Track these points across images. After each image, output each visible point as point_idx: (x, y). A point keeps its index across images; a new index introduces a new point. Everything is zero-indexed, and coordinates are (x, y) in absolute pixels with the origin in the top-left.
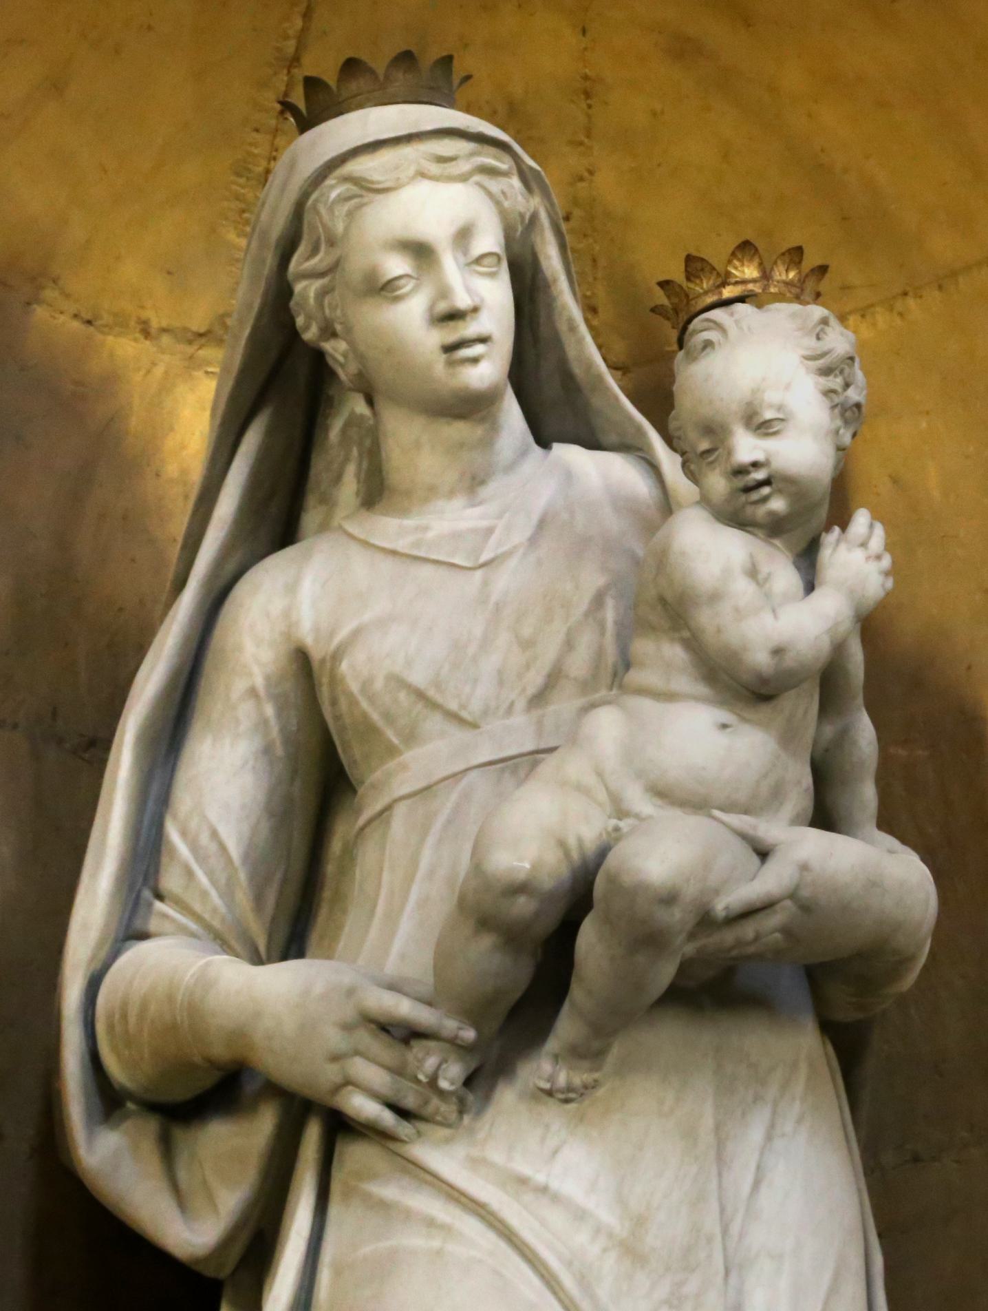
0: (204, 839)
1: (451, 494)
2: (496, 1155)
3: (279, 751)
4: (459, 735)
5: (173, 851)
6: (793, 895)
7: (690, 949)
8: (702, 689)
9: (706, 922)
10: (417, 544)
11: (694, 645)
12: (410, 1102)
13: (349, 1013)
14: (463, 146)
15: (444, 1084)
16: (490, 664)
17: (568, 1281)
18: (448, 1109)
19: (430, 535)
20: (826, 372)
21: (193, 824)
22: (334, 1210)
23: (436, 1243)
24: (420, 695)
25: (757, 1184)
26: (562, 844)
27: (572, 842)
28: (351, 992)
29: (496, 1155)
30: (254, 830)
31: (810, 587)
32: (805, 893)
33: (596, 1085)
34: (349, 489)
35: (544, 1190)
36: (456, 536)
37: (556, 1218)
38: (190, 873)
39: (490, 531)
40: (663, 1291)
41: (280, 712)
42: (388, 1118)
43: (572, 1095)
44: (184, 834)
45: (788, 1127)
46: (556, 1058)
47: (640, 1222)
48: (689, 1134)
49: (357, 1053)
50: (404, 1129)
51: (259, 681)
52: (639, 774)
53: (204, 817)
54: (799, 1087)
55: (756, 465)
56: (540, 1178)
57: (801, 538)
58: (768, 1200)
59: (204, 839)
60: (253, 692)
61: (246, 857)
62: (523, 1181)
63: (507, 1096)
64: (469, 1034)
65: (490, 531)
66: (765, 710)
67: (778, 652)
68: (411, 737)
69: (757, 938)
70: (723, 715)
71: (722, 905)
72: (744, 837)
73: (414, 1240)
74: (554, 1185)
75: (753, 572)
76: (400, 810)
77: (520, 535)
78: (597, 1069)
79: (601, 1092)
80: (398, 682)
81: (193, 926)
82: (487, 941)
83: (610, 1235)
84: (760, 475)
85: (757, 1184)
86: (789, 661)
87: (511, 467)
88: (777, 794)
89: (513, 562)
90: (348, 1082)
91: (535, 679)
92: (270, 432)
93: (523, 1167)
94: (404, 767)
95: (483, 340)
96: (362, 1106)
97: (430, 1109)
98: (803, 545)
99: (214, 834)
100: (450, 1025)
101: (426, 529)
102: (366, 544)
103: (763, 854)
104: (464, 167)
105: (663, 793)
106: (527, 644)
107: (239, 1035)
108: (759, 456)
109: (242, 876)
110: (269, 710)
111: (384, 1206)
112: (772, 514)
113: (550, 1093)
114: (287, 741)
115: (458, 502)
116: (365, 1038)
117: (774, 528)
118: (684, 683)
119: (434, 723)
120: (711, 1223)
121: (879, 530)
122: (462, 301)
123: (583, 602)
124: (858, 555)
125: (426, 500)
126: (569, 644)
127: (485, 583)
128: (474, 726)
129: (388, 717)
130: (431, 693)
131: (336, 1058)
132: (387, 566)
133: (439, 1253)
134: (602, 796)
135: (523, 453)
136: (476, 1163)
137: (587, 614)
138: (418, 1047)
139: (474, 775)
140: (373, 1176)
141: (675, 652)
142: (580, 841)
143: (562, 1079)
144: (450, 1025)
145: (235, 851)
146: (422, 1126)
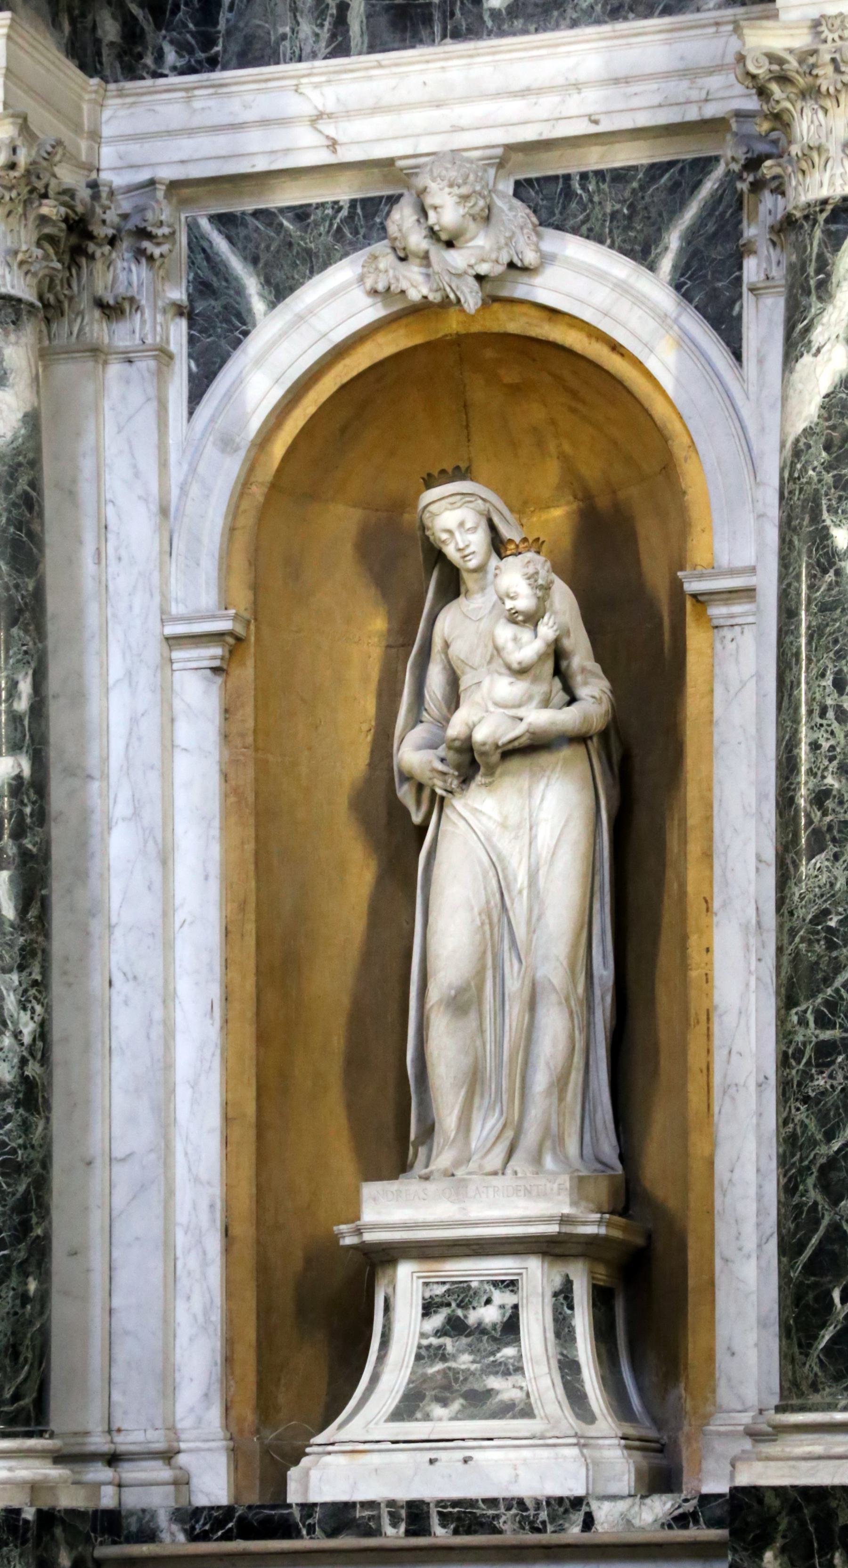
2: (470, 802)
14: (459, 497)
17: (482, 838)
28: (431, 762)
29: (470, 802)
37: (484, 820)
45: (553, 781)
47: (506, 818)
48: (520, 791)
54: (558, 769)
58: (546, 804)
63: (473, 785)
70: (512, 679)
88: (530, 698)
89: (484, 620)
95: (473, 553)
103: (521, 719)
104: (459, 504)
105: (496, 704)
116: (436, 774)
120: (526, 815)
122: (461, 546)
136: (466, 805)
144: (451, 771)
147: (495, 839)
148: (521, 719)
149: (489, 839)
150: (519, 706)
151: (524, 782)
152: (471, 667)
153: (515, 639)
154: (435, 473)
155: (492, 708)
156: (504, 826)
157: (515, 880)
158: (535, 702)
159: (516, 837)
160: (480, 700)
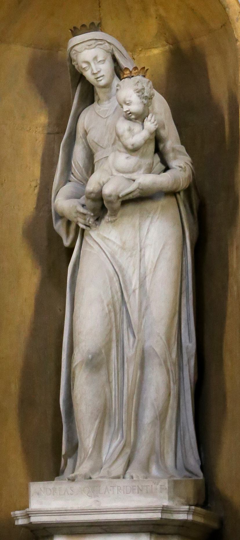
0: (77, 163)
6: (138, 188)
16: (107, 137)
20: (138, 92)
25: (148, 233)
30: (84, 161)
32: (140, 188)
33: (116, 220)
35: (108, 239)
40: (129, 254)
46: (109, 216)
47: (124, 243)
53: (76, 160)
55: (128, 111)
56: (107, 237)
58: (150, 235)
63: (103, 222)
67: (133, 145)
70: (128, 155)
71: (120, 196)
74: (110, 238)
78: (116, 217)
79: (117, 220)
80: (93, 140)
84: (128, 113)
85: (148, 233)
88: (140, 167)
92: (82, 86)
93: (105, 236)
95: (103, 76)
103: (134, 181)
105: (118, 171)
108: (128, 109)
115: (107, 102)
116: (79, 215)
117: (136, 119)
118: (122, 149)
119: (99, 148)
131: (75, 218)
136: (98, 235)
144: (89, 213)
145: (81, 166)
148: (134, 181)
149: (114, 257)
150: (133, 172)
153: (130, 130)
154: (79, 27)
155: (115, 173)
156: (123, 248)
157: (131, 283)
158: (142, 171)
159: (131, 256)
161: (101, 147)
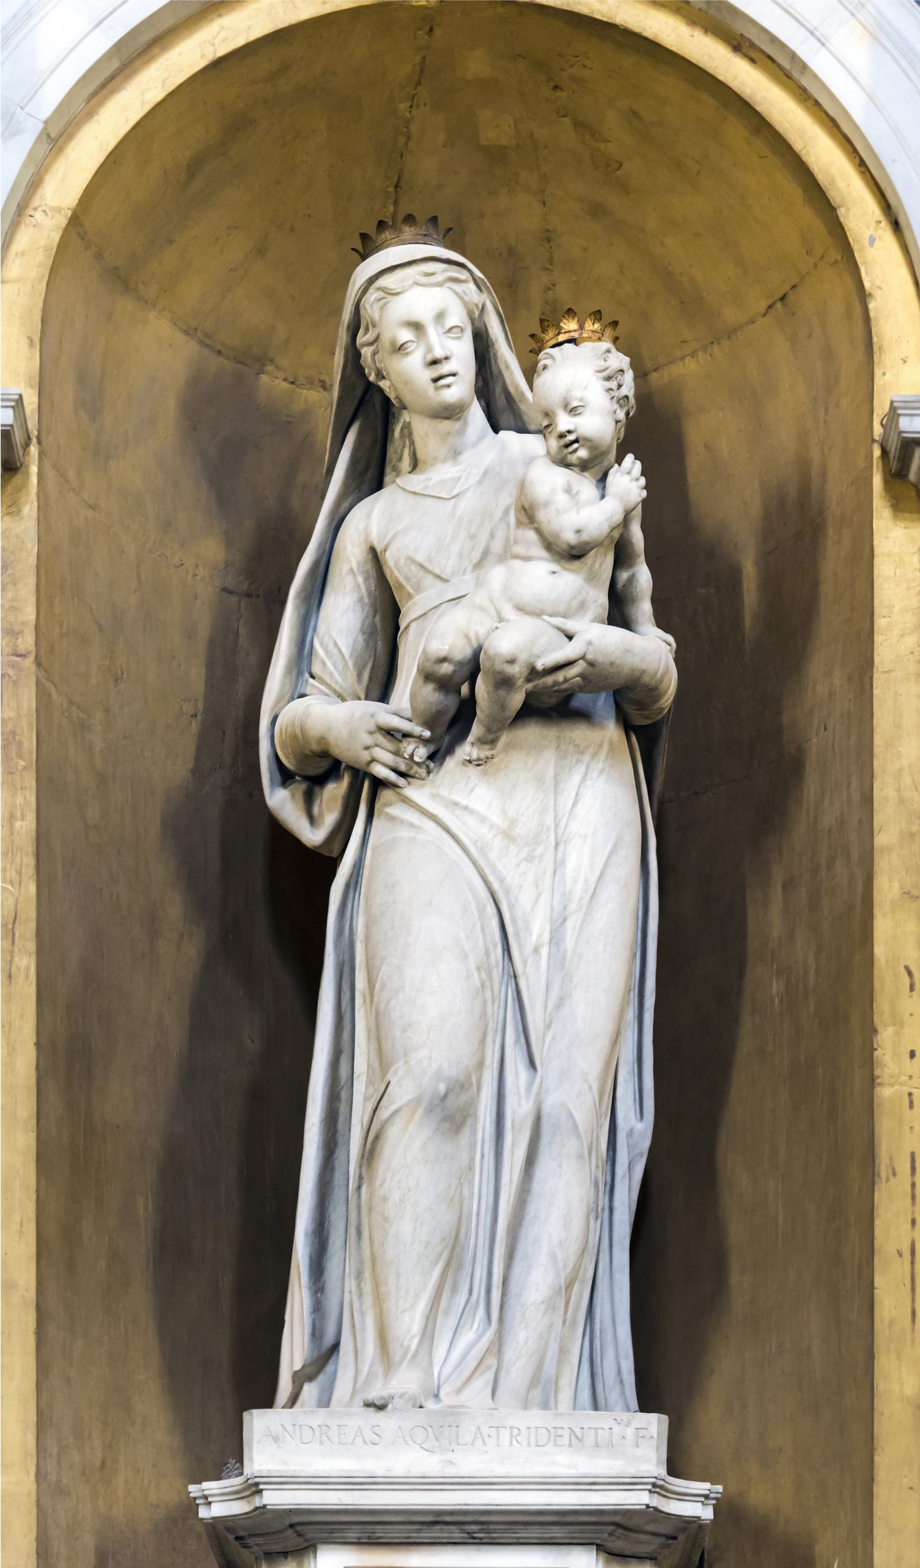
0: (331, 646)
1: (445, 460)
2: (444, 792)
3: (366, 600)
4: (439, 585)
5: (317, 654)
6: (583, 658)
7: (530, 686)
8: (544, 553)
9: (533, 673)
10: (425, 488)
11: (538, 531)
12: (403, 768)
13: (372, 727)
15: (416, 759)
16: (455, 549)
17: (473, 850)
18: (422, 772)
19: (431, 483)
21: (326, 639)
22: (375, 821)
23: (412, 835)
24: (422, 566)
26: (467, 636)
27: (472, 636)
28: (372, 716)
31: (603, 497)
32: (589, 656)
34: (406, 463)
35: (466, 808)
36: (443, 482)
37: (471, 821)
38: (324, 664)
39: (459, 478)
40: (524, 854)
41: (366, 579)
42: (393, 777)
43: (480, 762)
44: (322, 644)
47: (513, 822)
48: (540, 780)
49: (377, 745)
50: (401, 781)
51: (354, 565)
52: (510, 600)
55: (569, 432)
56: (464, 802)
57: (598, 470)
59: (331, 646)
60: (352, 570)
61: (352, 655)
62: (456, 804)
63: (451, 763)
64: (427, 734)
65: (459, 478)
66: (576, 564)
68: (418, 589)
69: (566, 681)
70: (555, 567)
71: (540, 665)
72: (559, 629)
73: (404, 833)
74: (471, 805)
75: (568, 491)
76: (413, 626)
77: (473, 481)
79: (495, 760)
80: (413, 561)
81: (326, 690)
82: (430, 687)
83: (498, 829)
84: (571, 437)
86: (585, 537)
87: (475, 445)
88: (582, 606)
89: (469, 494)
90: (373, 760)
91: (476, 556)
93: (457, 798)
94: (415, 604)
96: (381, 771)
97: (412, 772)
98: (600, 475)
99: (336, 644)
100: (417, 729)
101: (429, 479)
102: (403, 489)
103: (570, 638)
105: (521, 609)
106: (473, 537)
107: (322, 740)
108: (571, 427)
109: (350, 664)
110: (360, 579)
111: (393, 819)
112: (579, 458)
113: (470, 762)
114: (370, 596)
116: (380, 738)
117: (584, 466)
119: (429, 580)
120: (549, 820)
121: (638, 465)
123: (499, 514)
124: (626, 478)
125: (433, 465)
126: (492, 536)
127: (455, 506)
128: (447, 581)
129: (408, 579)
130: (427, 565)
131: (367, 748)
132: (412, 499)
133: (413, 839)
134: (493, 612)
135: (481, 438)
136: (435, 796)
137: (501, 519)
138: (405, 743)
139: (444, 606)
140: (389, 804)
141: (531, 535)
142: (477, 634)
143: (475, 756)
144: (417, 729)
145: (346, 653)
146: (410, 780)
147: (493, 855)
151: (548, 761)
152: (438, 577)
156: (508, 836)
158: (590, 615)
159: (529, 859)
160: (487, 604)
161: (438, 577)
